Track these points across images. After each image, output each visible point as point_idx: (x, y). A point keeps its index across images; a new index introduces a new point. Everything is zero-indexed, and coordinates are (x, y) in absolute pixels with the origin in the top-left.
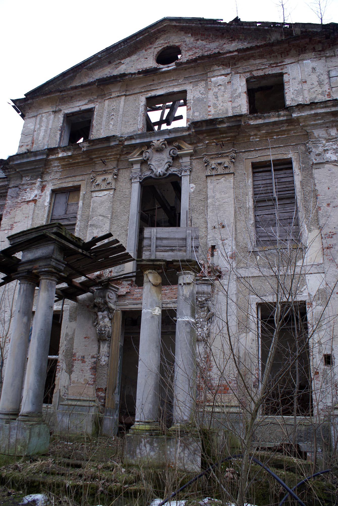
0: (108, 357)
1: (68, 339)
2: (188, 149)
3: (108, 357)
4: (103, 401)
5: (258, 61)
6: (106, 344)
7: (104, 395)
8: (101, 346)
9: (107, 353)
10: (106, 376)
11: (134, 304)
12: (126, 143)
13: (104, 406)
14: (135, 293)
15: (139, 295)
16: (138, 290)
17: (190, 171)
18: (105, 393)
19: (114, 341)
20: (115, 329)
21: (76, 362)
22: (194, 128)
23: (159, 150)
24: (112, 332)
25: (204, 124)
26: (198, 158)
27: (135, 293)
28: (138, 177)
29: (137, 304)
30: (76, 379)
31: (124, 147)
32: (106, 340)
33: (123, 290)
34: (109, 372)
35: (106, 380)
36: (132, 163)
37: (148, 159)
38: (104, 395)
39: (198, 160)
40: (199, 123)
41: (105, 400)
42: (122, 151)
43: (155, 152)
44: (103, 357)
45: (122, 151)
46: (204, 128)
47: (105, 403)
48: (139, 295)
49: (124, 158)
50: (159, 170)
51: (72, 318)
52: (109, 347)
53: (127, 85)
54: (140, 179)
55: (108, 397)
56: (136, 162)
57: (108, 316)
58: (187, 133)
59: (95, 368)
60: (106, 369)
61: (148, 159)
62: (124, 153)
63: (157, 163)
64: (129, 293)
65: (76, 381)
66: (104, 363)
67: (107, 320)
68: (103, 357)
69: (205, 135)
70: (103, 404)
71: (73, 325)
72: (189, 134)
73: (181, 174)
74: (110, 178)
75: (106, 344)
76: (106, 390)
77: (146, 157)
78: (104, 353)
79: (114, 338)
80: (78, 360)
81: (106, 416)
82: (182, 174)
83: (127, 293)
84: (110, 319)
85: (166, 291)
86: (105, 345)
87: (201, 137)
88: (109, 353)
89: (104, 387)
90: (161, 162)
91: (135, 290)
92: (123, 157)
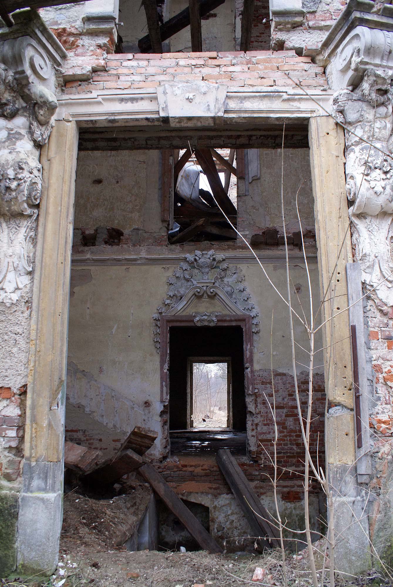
0: (30, 273)
3: (30, 273)
4: (12, 433)
6: (23, 230)
7: (18, 412)
9: (24, 263)
10: (22, 343)
13: (18, 451)
14: (125, 71)
15: (137, 78)
16: (134, 63)
18: (22, 405)
19: (50, 217)
20: (53, 180)
24: (46, 189)
27: (121, 71)
32: (21, 215)
33: (80, 62)
34: (33, 326)
35: (23, 356)
38: (18, 412)
41: (21, 428)
44: (11, 276)
47: (21, 439)
48: (137, 78)
52: (34, 241)
55: (34, 420)
57: (31, 132)
60: (22, 317)
64: (104, 69)
66: (15, 297)
67: (25, 146)
68: (11, 276)
70: (14, 444)
75: (23, 230)
76: (23, 392)
78: (15, 259)
79: (51, 210)
81: (28, 489)
83: (95, 71)
84: (39, 146)
85: (231, 69)
86: (16, 233)
88: (32, 261)
89: (15, 384)
91: (125, 64)
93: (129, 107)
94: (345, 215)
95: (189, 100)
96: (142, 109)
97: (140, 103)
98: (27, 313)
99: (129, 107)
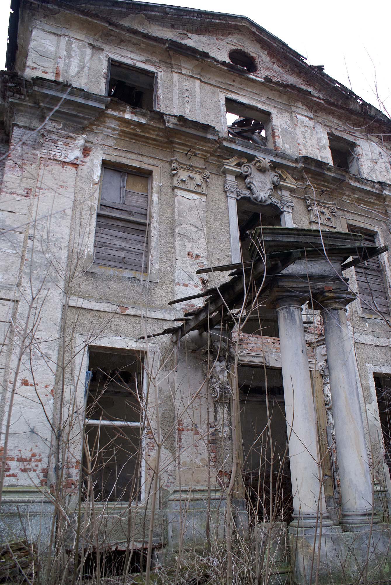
1: (163, 396)
2: (290, 183)
5: (335, 121)
8: (219, 410)
11: (253, 356)
12: (225, 144)
14: (250, 342)
15: (254, 345)
16: (252, 339)
17: (292, 209)
21: (185, 432)
22: (303, 163)
23: (262, 170)
25: (313, 164)
26: (297, 197)
28: (235, 192)
29: (257, 357)
30: (189, 459)
31: (219, 147)
36: (225, 172)
37: (247, 176)
39: (297, 200)
40: (310, 161)
42: (216, 151)
43: (257, 171)
45: (216, 151)
46: (313, 168)
48: (254, 345)
49: (212, 160)
50: (262, 195)
51: (168, 365)
53: (202, 69)
54: (237, 196)
56: (232, 172)
58: (294, 165)
59: (214, 443)
61: (247, 176)
62: (216, 154)
63: (260, 185)
65: (188, 463)
69: (310, 175)
71: (174, 377)
72: (296, 168)
73: (283, 208)
74: (198, 179)
77: (247, 172)
80: (188, 430)
82: (285, 209)
87: (305, 176)
90: (265, 185)
91: (250, 338)
92: (212, 158)
93: (255, 360)
94: (324, 409)
95: (276, 360)
96: (259, 361)
97: (259, 358)
98: (230, 442)
99: (255, 360)
